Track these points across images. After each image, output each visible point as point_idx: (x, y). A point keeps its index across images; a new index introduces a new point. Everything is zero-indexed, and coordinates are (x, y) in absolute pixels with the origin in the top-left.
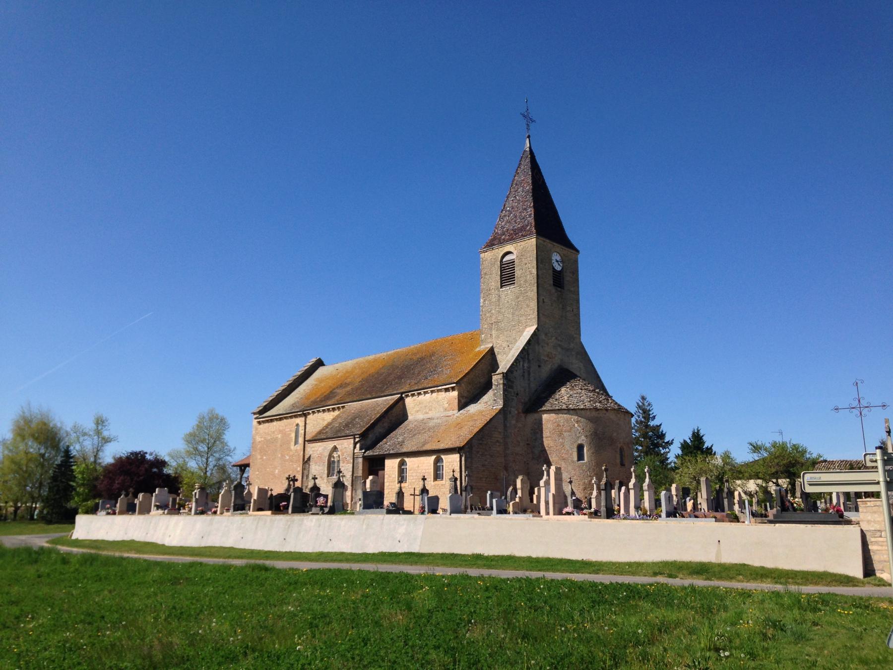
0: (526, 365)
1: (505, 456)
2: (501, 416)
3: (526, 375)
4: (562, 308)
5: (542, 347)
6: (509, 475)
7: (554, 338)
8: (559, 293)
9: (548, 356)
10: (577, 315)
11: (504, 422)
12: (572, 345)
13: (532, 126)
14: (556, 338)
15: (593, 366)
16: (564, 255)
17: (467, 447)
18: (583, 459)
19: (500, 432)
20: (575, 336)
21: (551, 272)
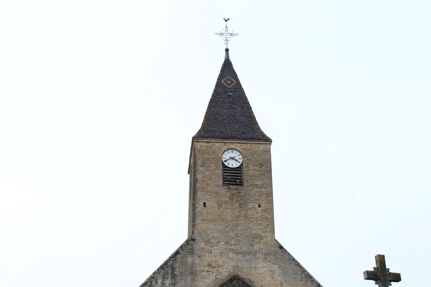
4: (240, 207)
5: (200, 257)
8: (235, 192)
9: (210, 265)
10: (270, 210)
12: (257, 247)
14: (227, 243)
15: (298, 265)
16: (244, 149)
20: (264, 234)
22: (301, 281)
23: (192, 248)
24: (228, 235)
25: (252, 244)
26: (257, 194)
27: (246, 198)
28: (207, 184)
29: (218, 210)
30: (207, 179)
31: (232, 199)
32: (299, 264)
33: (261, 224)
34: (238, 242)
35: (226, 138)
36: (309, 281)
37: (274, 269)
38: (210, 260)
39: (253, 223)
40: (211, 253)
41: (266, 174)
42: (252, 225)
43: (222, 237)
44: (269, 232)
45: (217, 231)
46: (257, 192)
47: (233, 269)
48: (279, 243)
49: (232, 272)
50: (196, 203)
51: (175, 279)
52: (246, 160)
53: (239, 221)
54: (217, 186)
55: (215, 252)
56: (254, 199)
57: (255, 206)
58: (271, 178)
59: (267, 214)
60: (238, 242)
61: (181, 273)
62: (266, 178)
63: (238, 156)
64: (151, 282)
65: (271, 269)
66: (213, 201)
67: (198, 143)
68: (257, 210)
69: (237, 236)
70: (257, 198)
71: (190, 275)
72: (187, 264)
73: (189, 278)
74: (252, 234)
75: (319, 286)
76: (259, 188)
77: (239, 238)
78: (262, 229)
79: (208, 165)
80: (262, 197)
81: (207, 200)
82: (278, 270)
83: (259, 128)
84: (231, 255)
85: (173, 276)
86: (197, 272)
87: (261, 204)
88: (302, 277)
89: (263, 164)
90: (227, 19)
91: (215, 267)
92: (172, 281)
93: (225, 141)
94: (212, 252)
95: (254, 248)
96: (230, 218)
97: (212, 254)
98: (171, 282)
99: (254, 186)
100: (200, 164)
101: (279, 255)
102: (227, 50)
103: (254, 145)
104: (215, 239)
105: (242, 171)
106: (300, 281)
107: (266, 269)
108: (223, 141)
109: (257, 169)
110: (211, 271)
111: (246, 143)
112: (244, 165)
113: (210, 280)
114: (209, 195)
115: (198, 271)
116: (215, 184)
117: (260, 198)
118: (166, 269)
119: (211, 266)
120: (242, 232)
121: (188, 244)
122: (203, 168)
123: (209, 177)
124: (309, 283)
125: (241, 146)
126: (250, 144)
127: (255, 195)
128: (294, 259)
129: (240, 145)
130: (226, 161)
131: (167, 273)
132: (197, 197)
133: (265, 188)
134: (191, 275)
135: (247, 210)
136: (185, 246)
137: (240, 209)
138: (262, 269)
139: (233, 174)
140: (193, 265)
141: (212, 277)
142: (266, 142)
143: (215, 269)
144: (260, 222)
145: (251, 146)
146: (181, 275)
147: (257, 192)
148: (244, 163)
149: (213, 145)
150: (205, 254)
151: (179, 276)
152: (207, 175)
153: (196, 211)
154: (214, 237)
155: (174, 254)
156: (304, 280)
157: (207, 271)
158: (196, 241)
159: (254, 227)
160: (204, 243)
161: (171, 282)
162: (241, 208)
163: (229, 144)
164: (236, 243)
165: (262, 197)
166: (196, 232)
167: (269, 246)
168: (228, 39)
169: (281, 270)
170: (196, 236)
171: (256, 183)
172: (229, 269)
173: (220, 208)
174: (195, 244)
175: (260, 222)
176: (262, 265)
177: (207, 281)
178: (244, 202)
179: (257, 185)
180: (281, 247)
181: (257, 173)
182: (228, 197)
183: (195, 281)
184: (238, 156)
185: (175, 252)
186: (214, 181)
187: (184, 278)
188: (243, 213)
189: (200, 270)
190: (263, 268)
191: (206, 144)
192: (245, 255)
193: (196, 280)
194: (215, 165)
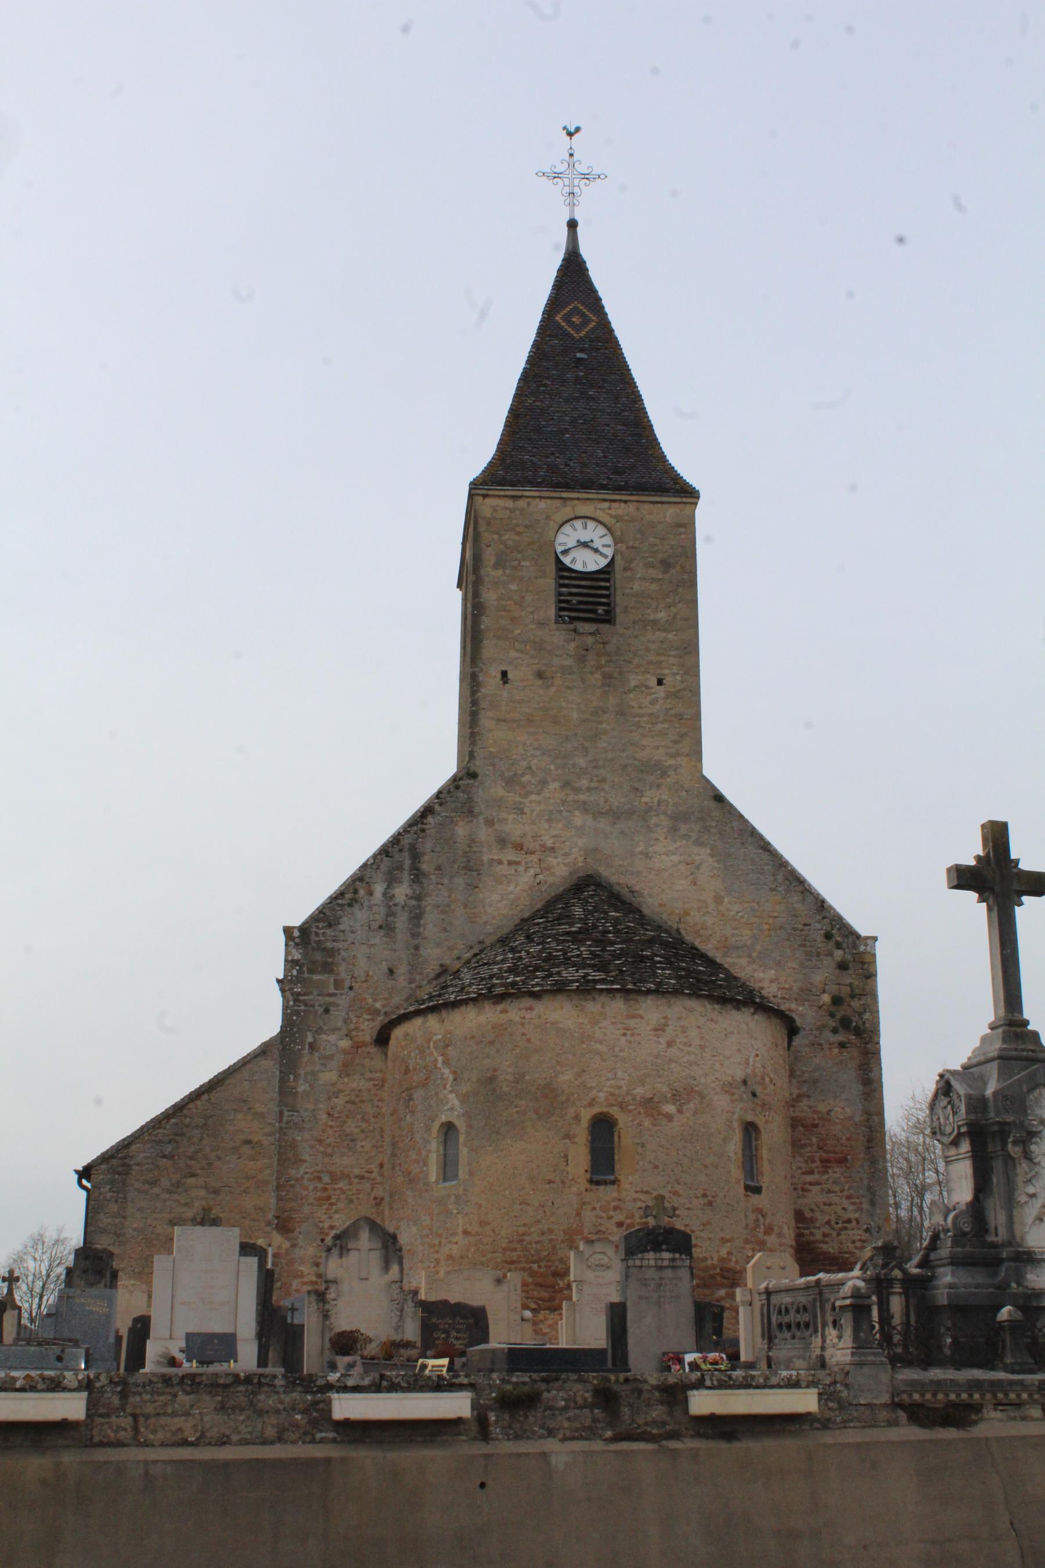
0: (402, 892)
1: (279, 1187)
2: (269, 1065)
3: (401, 922)
4: (603, 685)
5: (490, 823)
6: (293, 1246)
7: (554, 785)
8: (590, 640)
11: (283, 1081)
12: (650, 796)
13: (588, 193)
14: (566, 784)
15: (765, 846)
16: (618, 518)
17: (103, 1167)
18: (455, 1177)
19: (262, 1115)
21: (549, 582)
22: (774, 893)
23: (470, 799)
24: (571, 762)
25: (637, 789)
26: (653, 647)
27: (623, 658)
28: (513, 619)
29: (541, 692)
30: (512, 603)
31: (582, 660)
32: (769, 844)
33: (663, 734)
34: (599, 781)
35: (566, 486)
36: (795, 891)
37: (697, 858)
38: (518, 832)
39: (640, 731)
40: (522, 813)
41: (680, 590)
42: (638, 737)
43: (552, 767)
44: (687, 755)
45: (538, 753)
46: (653, 642)
47: (582, 859)
48: (714, 788)
49: (580, 864)
50: (481, 670)
51: (421, 883)
52: (624, 548)
53: (601, 723)
54: (541, 624)
55: (532, 811)
56: (645, 662)
57: (647, 683)
58: (694, 602)
59: (680, 705)
60: (599, 781)
61: (439, 868)
62: (679, 602)
63: (601, 537)
64: (356, 892)
65: (689, 859)
66: (528, 665)
67: (487, 500)
68: (654, 693)
69: (596, 767)
70: (652, 657)
71: (463, 872)
72: (455, 843)
73: (459, 882)
74: (636, 759)
75: (823, 906)
76: (659, 630)
77: (602, 770)
78: (668, 747)
79: (515, 563)
80: (669, 656)
81: (510, 663)
82: (710, 860)
83: (662, 458)
84: (579, 819)
85: (416, 876)
86: (483, 864)
87: (664, 675)
88: (775, 880)
89: (672, 560)
90: (573, 130)
91: (533, 853)
92: (412, 889)
93: (564, 495)
94: (526, 810)
95: (644, 800)
96: (575, 715)
97: (524, 816)
98: (409, 892)
99: (645, 627)
100: (493, 560)
101: (713, 821)
102: (572, 225)
103: (647, 506)
104: (533, 774)
105: (612, 581)
106: (769, 893)
107: (675, 858)
108: (558, 495)
109: (656, 576)
110: (523, 863)
111: (625, 502)
112: (619, 563)
113: (519, 888)
114: (517, 651)
115: (485, 862)
116: (536, 617)
117: (663, 658)
118: (397, 856)
119: (522, 849)
120: (610, 756)
121: (457, 787)
122: (500, 572)
123: (516, 597)
124: (795, 898)
125: (610, 508)
126: (635, 504)
127: (648, 650)
128: (754, 833)
129: (606, 505)
130: (566, 552)
131: (400, 868)
132: (484, 657)
133: (676, 631)
134: (466, 874)
135: (625, 693)
136: (449, 792)
137: (607, 689)
138: (664, 857)
139: (585, 591)
140: (473, 845)
141: (526, 879)
142: (681, 497)
143: (534, 858)
144: (660, 726)
145: (638, 509)
146: (437, 872)
147: (653, 642)
148: (618, 558)
149: (529, 504)
150: (504, 815)
151: (432, 877)
152: (511, 591)
153: (479, 694)
154: (530, 768)
155: (419, 814)
156: (780, 889)
157: (510, 863)
158: (480, 778)
159: (644, 742)
160: (503, 784)
161: (409, 892)
162: (609, 686)
163: (576, 502)
164: (593, 785)
165: (669, 656)
166: (479, 753)
167: (685, 793)
168: (576, 190)
169: (718, 862)
170: (479, 765)
171: (652, 617)
172: (573, 856)
173: (548, 687)
174: (478, 787)
175: (660, 726)
176: (665, 847)
177: (511, 888)
178: (617, 670)
179: (654, 622)
180: (719, 798)
181: (654, 587)
182: (571, 656)
183: (477, 890)
184: (601, 537)
185: (422, 810)
186: (531, 609)
187: (446, 881)
188: (612, 701)
189: (492, 859)
190: (668, 856)
191: (510, 504)
192: (619, 818)
193: (481, 886)
194: (533, 563)
